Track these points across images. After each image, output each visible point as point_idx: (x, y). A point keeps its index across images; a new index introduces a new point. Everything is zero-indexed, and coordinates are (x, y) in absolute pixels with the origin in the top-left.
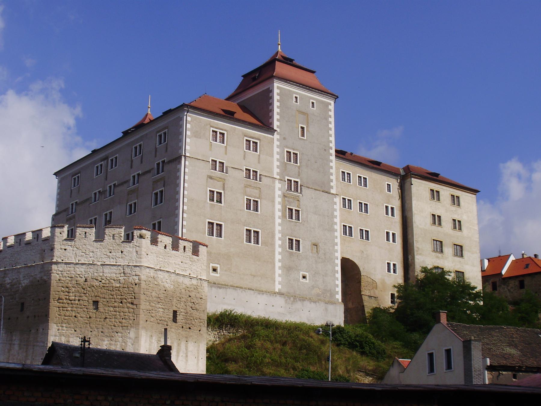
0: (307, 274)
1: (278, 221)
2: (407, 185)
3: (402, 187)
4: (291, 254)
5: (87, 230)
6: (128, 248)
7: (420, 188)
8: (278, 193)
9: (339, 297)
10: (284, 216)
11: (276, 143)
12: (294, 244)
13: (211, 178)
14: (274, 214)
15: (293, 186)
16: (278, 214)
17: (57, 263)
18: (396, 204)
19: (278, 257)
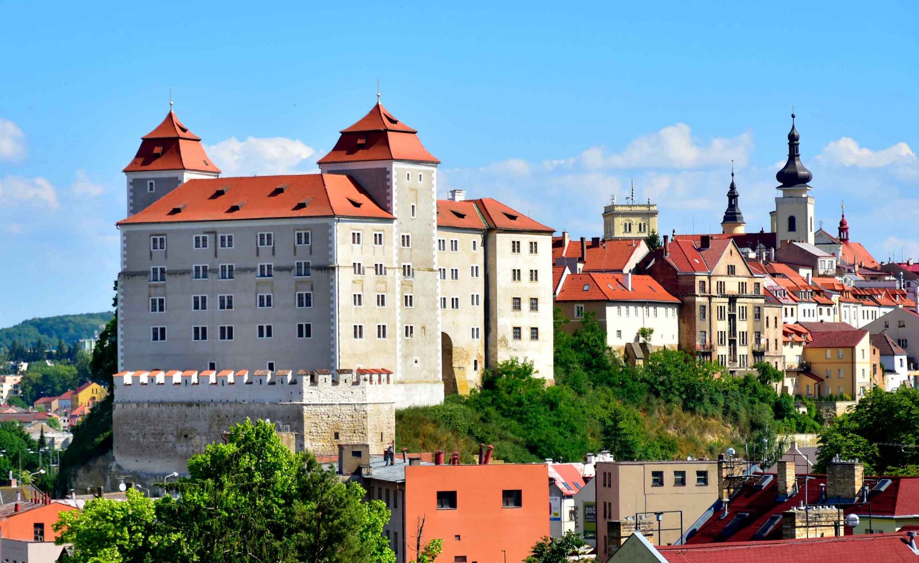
0: (418, 359)
1: (398, 310)
2: (490, 240)
3: (485, 244)
4: (407, 341)
5: (326, 376)
6: (356, 389)
7: (503, 241)
8: (398, 282)
9: (440, 376)
10: (402, 305)
11: (395, 230)
12: (409, 331)
13: (354, 282)
14: (395, 304)
15: (407, 271)
16: (398, 304)
17: (306, 405)
18: (480, 263)
19: (399, 346)
